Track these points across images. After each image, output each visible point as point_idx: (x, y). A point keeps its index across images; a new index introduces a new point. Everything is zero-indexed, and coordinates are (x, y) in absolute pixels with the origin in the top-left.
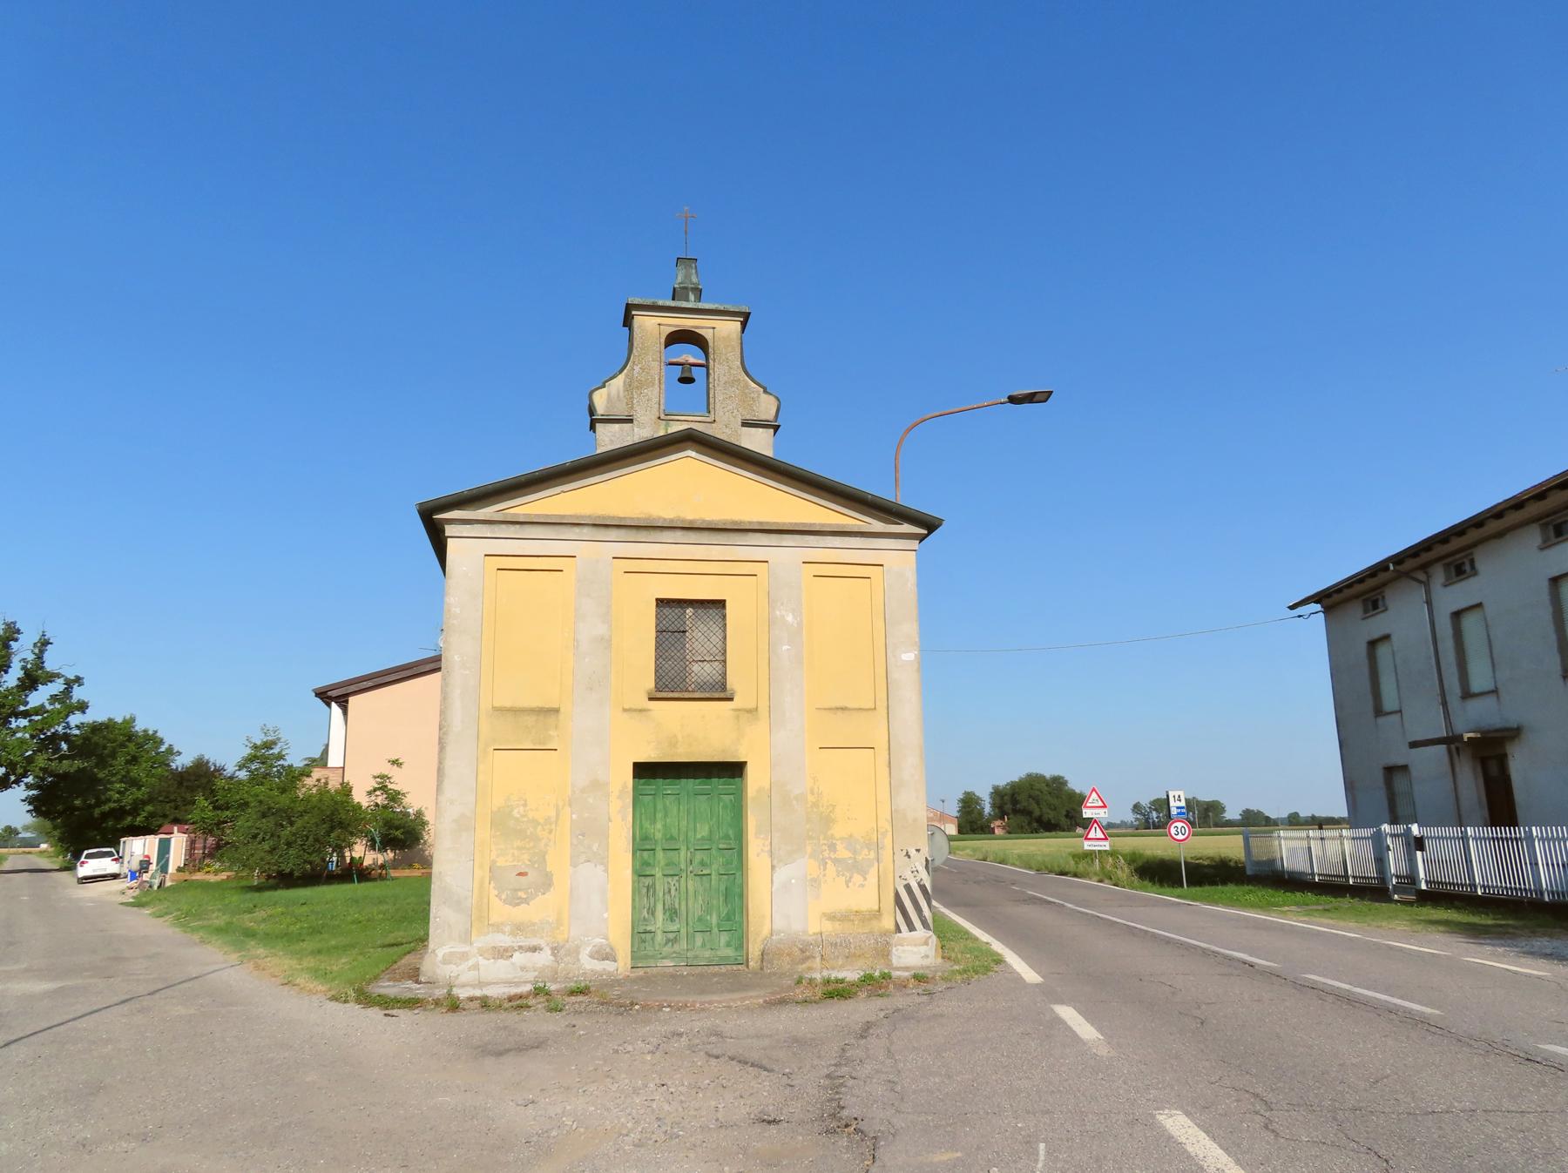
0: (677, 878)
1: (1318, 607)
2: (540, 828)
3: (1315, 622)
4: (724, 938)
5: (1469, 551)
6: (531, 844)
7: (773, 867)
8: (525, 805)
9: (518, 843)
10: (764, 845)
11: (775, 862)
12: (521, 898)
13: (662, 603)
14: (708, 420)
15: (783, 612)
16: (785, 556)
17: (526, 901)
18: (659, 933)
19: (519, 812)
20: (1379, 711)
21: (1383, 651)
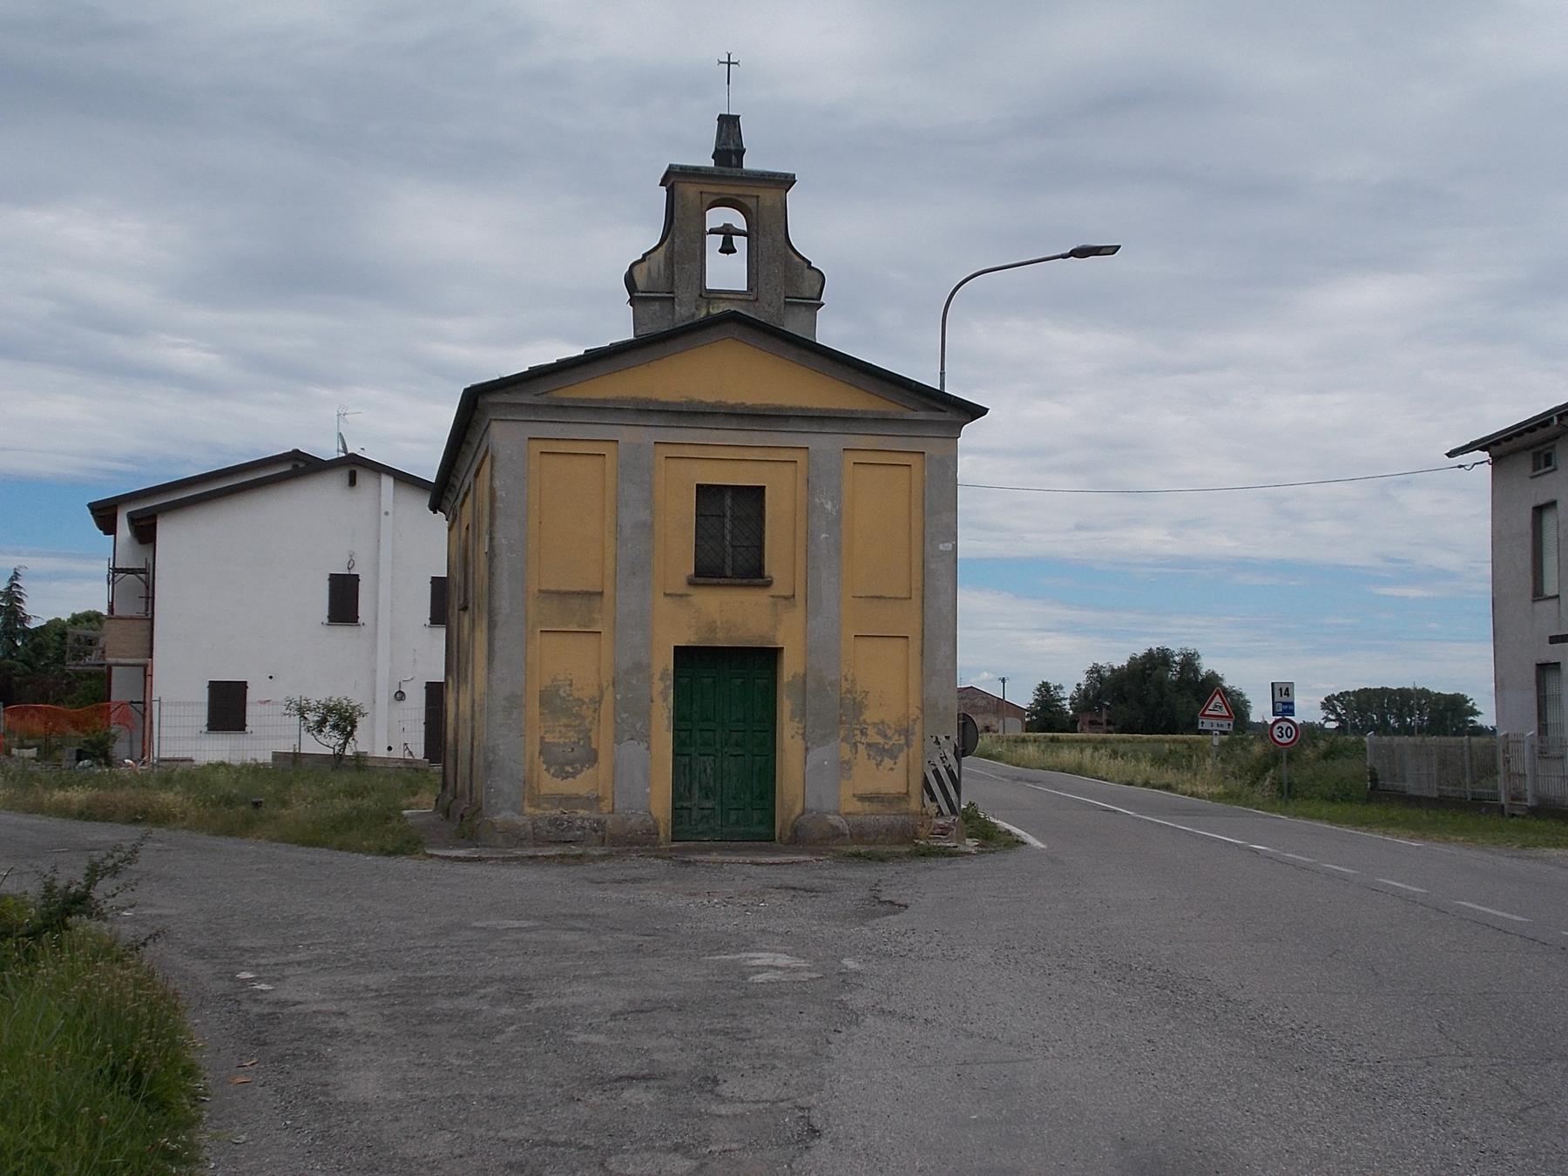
0: (712, 758)
1: (1485, 455)
2: (585, 706)
3: (1480, 469)
4: (757, 816)
5: (1553, 443)
6: (577, 723)
7: (807, 749)
8: (571, 685)
9: (564, 721)
10: (798, 728)
11: (809, 744)
12: (568, 772)
13: (701, 489)
14: (751, 298)
15: (824, 501)
16: (824, 444)
17: (573, 775)
18: (695, 809)
19: (565, 692)
20: (1538, 594)
21: (1549, 520)
